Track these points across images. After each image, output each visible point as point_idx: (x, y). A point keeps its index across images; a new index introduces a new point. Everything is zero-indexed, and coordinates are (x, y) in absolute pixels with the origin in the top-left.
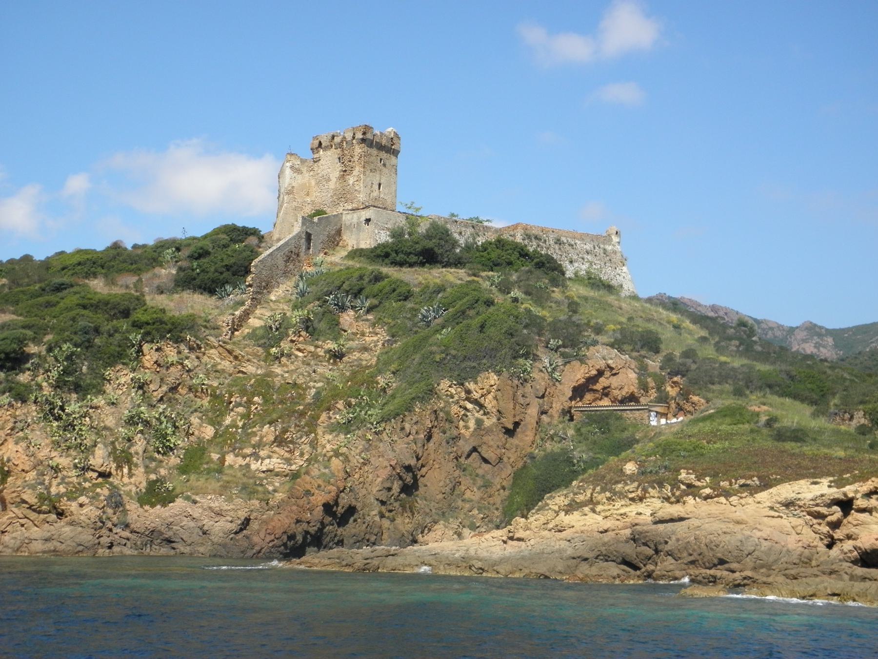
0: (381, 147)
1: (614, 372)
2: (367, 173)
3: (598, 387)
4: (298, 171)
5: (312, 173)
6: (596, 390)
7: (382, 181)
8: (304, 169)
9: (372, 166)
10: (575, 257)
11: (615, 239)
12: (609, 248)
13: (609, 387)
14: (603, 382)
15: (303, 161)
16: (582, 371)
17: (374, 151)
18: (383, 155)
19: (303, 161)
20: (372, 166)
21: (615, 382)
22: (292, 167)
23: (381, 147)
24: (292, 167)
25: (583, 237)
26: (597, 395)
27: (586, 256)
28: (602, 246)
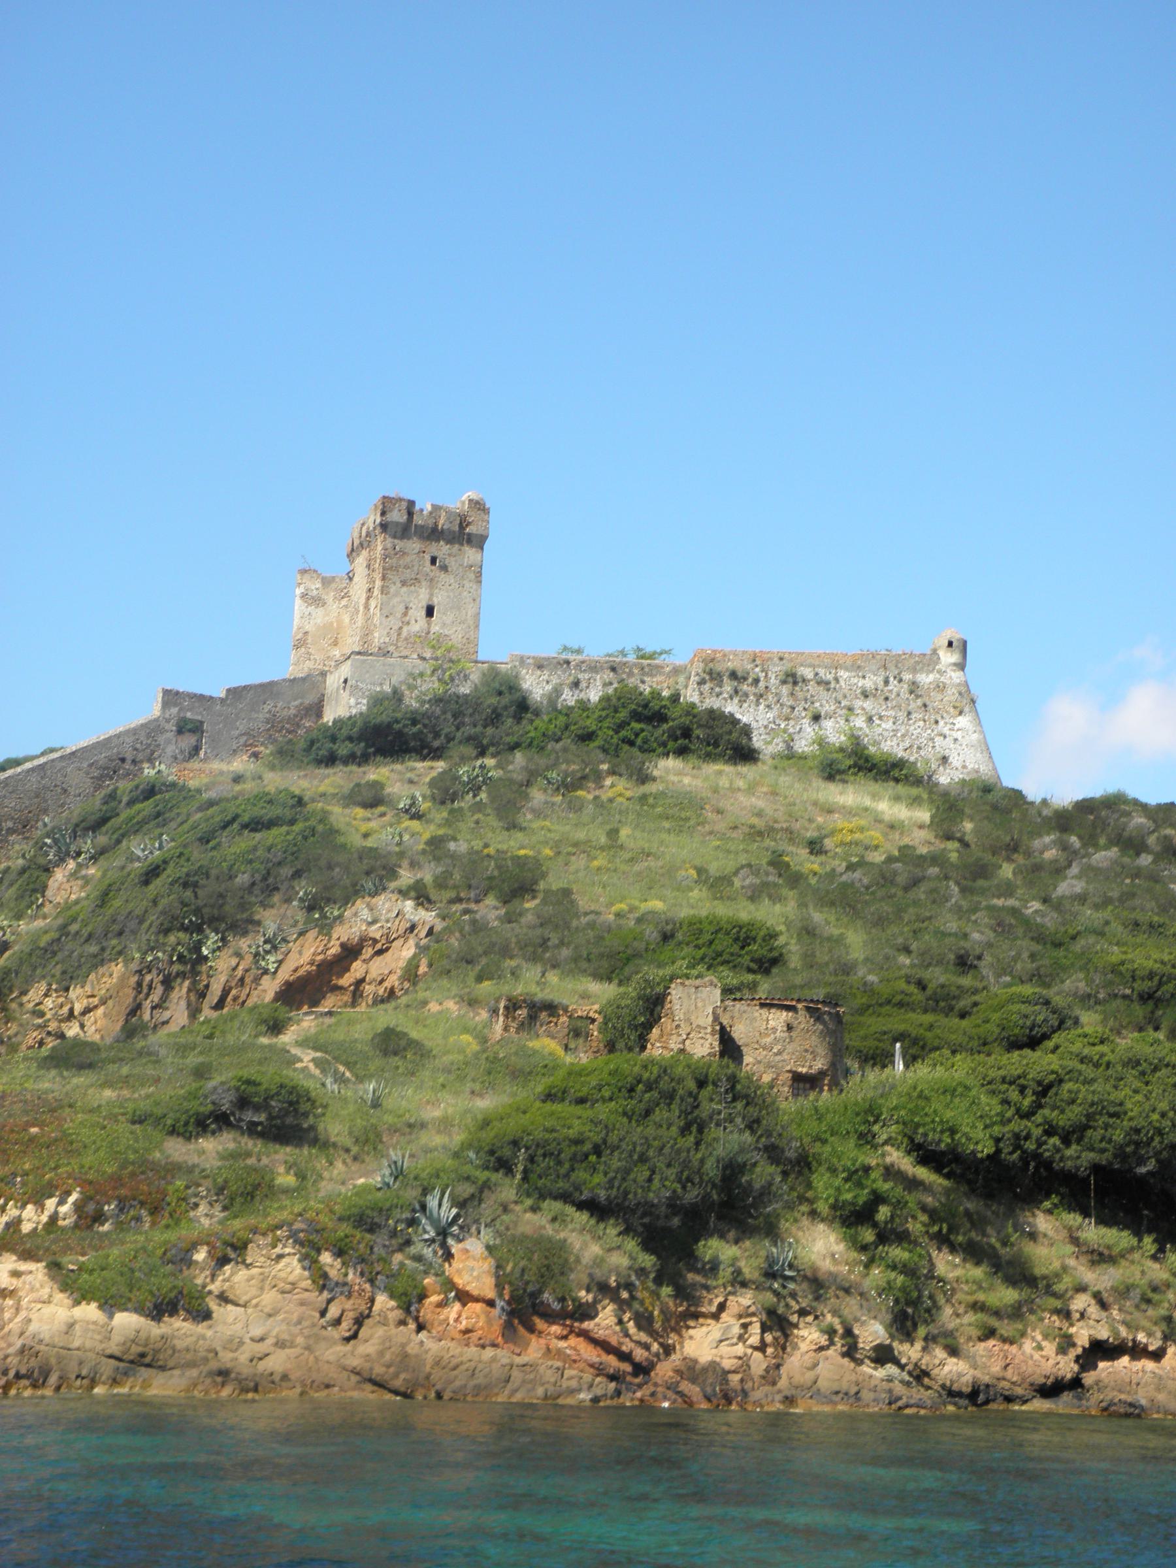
0: (433, 534)
1: (378, 946)
2: (393, 589)
3: (346, 980)
4: (316, 601)
5: (344, 602)
6: (341, 988)
7: (435, 601)
8: (329, 597)
9: (408, 574)
10: (827, 708)
11: (948, 658)
12: (926, 679)
13: (363, 980)
14: (358, 968)
15: (327, 582)
16: (312, 950)
17: (413, 545)
18: (442, 549)
19: (327, 582)
20: (408, 574)
21: (377, 967)
22: (304, 596)
23: (433, 534)
24: (304, 596)
25: (857, 665)
26: (345, 998)
27: (858, 703)
28: (907, 677)
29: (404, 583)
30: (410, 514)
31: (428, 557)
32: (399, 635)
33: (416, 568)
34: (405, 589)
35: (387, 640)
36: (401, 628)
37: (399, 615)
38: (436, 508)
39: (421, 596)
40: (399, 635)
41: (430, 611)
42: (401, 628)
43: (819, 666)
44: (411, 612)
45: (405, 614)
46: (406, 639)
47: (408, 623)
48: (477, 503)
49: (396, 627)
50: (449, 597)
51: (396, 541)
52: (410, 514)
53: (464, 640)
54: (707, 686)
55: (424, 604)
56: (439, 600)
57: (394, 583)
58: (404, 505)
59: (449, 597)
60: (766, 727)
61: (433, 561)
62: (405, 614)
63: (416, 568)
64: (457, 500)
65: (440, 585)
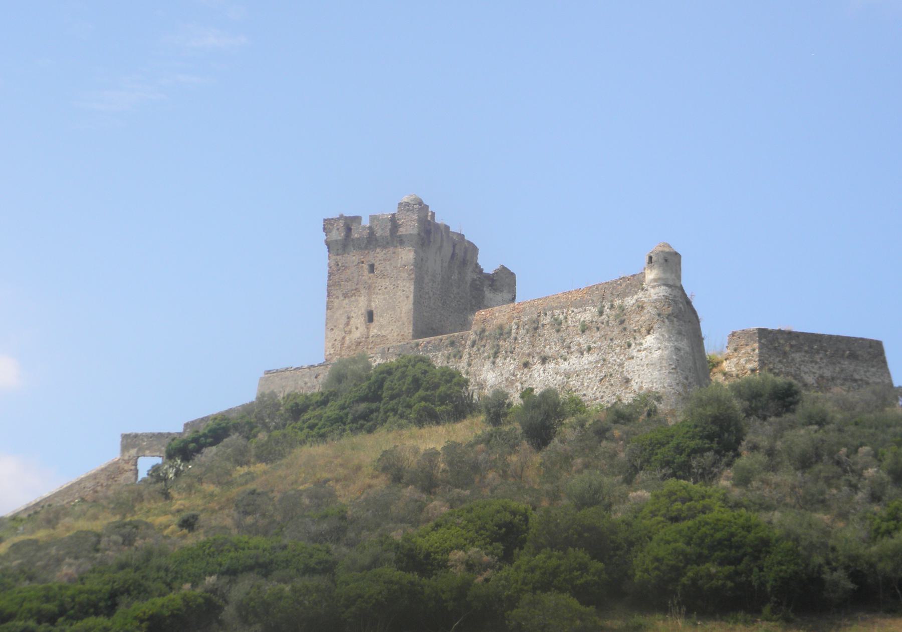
2: (336, 302)
17: (353, 257)
29: (345, 296)
30: (349, 230)
31: (366, 266)
32: (342, 344)
33: (355, 280)
34: (347, 301)
35: (332, 351)
36: (344, 338)
37: (341, 326)
38: (373, 218)
39: (361, 304)
40: (342, 344)
41: (370, 316)
42: (344, 338)
43: (556, 308)
44: (352, 321)
45: (347, 324)
46: (349, 347)
47: (350, 332)
48: (407, 204)
49: (339, 338)
50: (385, 299)
51: (338, 257)
52: (349, 230)
53: (400, 338)
54: (475, 348)
55: (363, 310)
56: (377, 303)
57: (338, 297)
58: (341, 223)
59: (385, 299)
60: (507, 380)
61: (372, 268)
62: (347, 324)
63: (355, 280)
64: (389, 209)
65: (377, 290)
